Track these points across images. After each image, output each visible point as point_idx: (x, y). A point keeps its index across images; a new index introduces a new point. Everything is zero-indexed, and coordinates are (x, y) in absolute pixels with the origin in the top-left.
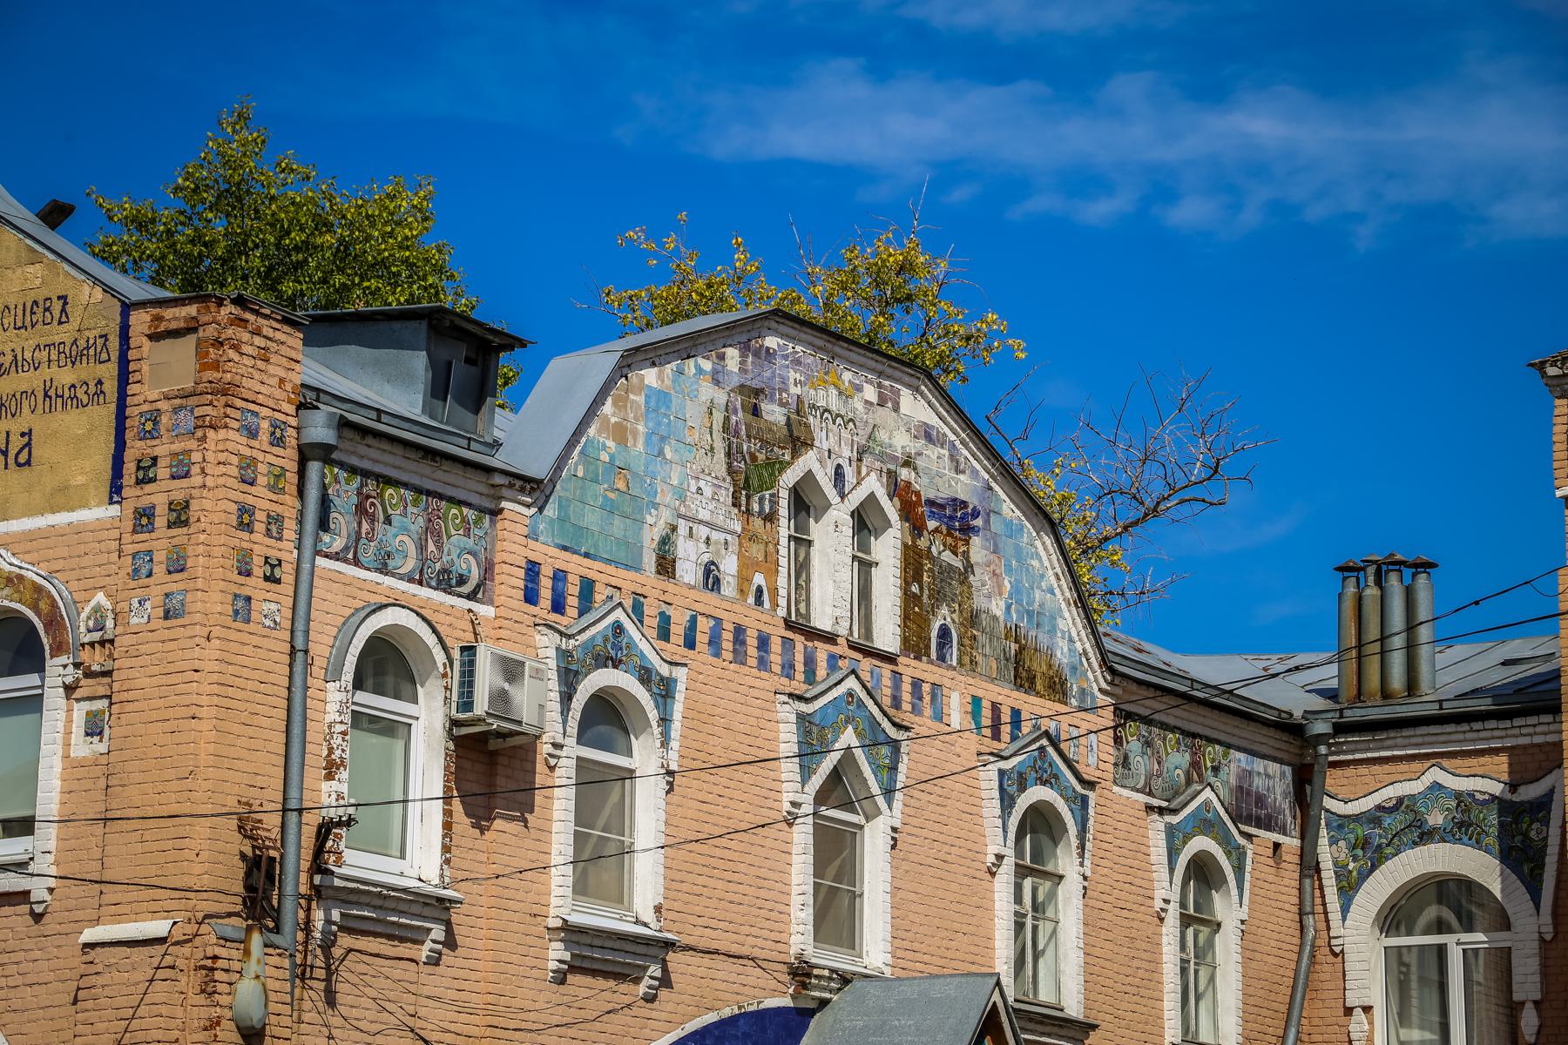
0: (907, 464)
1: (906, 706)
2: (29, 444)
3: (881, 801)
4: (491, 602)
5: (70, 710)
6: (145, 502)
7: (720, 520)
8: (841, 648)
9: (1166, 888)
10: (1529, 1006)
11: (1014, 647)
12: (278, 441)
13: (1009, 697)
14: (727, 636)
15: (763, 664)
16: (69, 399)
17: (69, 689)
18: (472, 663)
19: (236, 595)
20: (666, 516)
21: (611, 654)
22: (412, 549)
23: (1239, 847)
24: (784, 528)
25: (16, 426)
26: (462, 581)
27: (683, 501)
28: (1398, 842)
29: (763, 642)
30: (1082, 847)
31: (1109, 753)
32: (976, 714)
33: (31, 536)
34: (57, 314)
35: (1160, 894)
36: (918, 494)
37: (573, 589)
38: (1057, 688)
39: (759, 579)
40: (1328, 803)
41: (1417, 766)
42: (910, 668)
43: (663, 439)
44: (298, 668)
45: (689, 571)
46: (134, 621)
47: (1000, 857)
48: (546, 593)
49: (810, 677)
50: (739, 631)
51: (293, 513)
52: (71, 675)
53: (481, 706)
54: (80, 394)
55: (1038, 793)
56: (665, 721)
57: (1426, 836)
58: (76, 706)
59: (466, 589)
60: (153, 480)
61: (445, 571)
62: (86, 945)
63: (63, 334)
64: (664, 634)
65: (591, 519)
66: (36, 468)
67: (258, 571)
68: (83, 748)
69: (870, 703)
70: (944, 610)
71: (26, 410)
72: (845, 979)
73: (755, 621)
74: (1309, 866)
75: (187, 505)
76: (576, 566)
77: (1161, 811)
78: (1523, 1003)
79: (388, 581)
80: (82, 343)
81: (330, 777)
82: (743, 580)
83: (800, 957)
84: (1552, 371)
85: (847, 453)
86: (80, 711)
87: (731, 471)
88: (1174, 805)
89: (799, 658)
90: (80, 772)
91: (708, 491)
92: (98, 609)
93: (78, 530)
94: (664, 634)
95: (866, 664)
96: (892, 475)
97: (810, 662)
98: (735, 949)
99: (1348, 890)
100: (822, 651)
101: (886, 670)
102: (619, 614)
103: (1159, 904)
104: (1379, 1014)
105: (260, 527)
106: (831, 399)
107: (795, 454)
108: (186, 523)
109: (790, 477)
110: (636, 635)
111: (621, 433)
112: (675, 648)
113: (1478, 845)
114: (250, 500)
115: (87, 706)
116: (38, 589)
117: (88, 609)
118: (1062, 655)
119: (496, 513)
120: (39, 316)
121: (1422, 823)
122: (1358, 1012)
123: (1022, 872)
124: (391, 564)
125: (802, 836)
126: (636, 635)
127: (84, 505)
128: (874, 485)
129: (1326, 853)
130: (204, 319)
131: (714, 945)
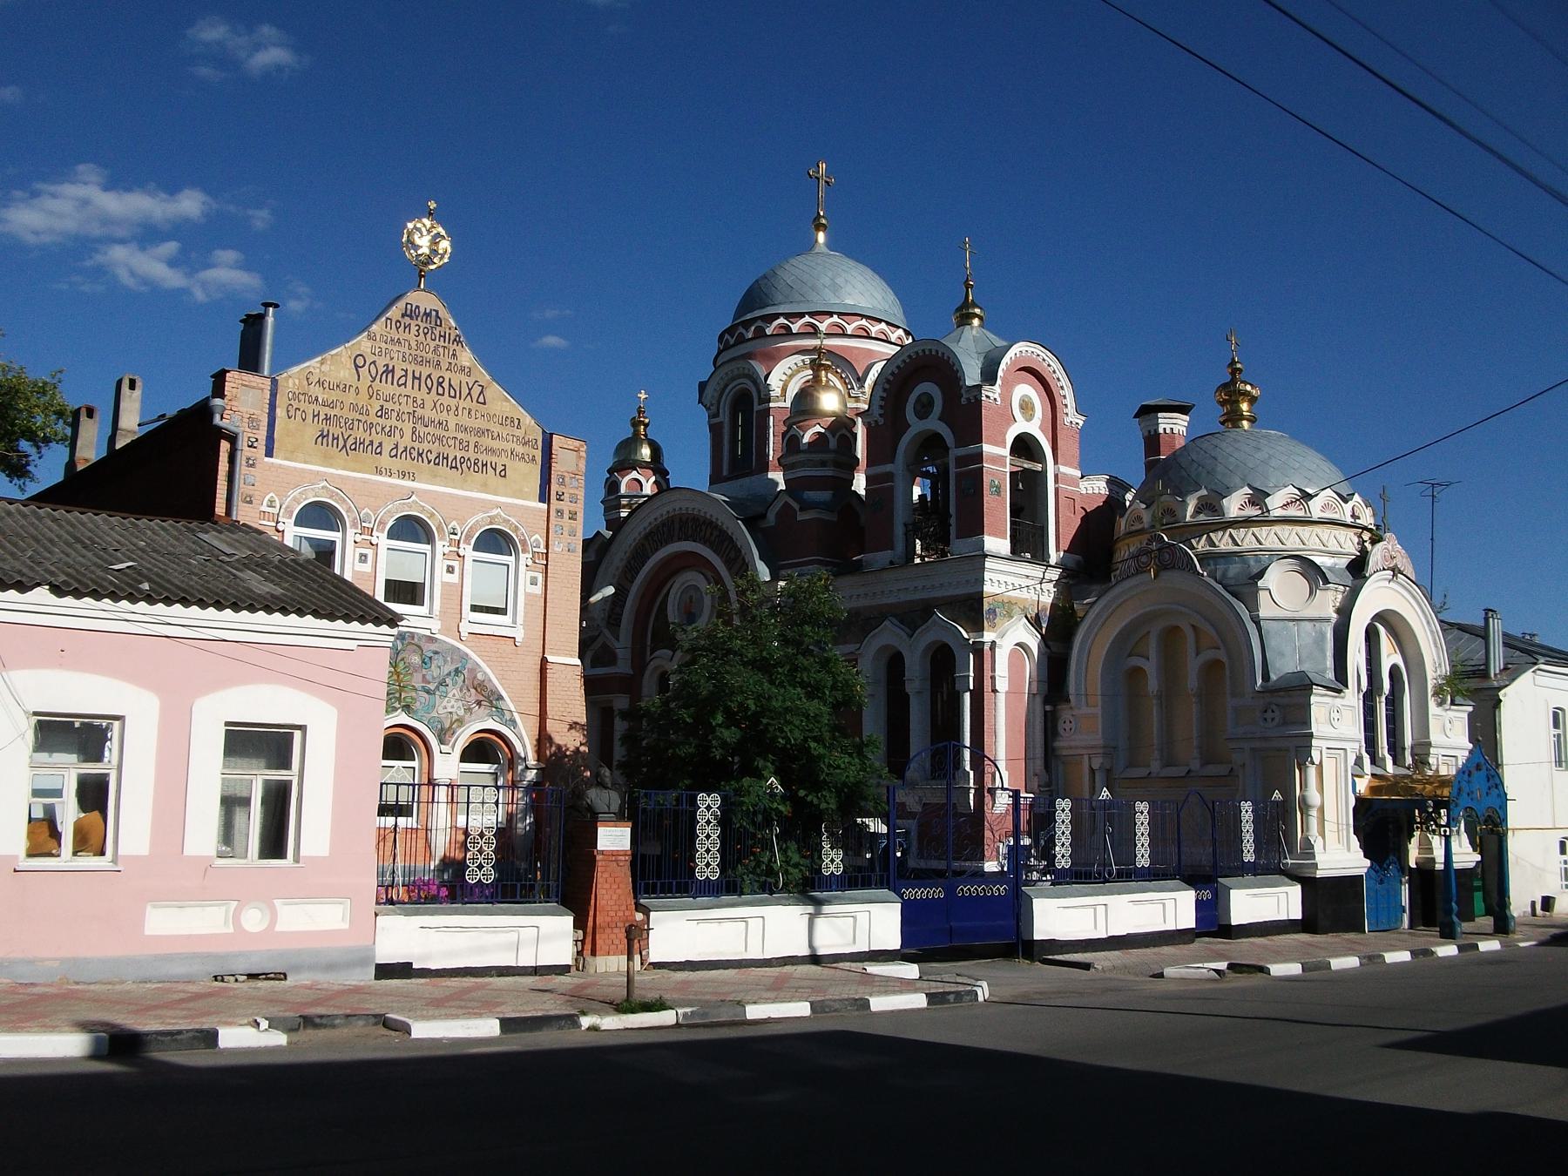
2: (505, 469)
6: (559, 507)
34: (516, 425)
54: (526, 457)
80: (527, 440)
92: (536, 540)
93: (527, 508)
108: (575, 520)
120: (509, 421)
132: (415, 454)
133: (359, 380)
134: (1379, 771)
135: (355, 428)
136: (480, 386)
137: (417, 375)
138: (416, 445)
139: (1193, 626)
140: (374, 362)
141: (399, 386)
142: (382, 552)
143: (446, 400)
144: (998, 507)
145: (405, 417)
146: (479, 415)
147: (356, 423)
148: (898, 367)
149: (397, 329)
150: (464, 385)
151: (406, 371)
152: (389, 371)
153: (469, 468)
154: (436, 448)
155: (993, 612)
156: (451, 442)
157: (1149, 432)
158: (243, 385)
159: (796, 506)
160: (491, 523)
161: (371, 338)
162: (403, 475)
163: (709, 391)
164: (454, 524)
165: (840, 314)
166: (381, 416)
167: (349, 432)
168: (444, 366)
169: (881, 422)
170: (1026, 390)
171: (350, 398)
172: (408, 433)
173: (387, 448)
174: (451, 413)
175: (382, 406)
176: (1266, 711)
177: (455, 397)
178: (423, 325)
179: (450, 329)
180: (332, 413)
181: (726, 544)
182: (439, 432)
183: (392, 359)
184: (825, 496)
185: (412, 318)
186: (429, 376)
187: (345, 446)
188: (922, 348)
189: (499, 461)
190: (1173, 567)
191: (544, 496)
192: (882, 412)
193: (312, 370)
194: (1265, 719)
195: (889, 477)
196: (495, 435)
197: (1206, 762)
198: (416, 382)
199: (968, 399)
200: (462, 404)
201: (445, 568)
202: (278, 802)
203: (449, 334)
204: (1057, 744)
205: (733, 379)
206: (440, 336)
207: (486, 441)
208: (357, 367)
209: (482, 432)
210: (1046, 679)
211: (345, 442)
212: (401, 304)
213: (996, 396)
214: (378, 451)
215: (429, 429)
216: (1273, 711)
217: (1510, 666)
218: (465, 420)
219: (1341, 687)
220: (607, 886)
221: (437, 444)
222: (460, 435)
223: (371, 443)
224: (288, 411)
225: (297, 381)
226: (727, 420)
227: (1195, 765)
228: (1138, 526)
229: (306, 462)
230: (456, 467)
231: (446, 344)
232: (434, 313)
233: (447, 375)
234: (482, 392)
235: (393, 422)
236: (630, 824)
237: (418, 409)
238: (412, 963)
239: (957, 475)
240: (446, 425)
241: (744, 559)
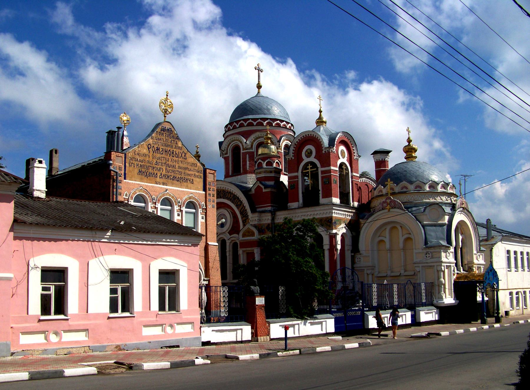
2: (193, 181)
63: (196, 168)
92: (203, 204)
93: (200, 194)
132: (167, 177)
134: (459, 272)
135: (149, 169)
137: (166, 150)
138: (167, 174)
139: (401, 227)
140: (154, 146)
141: (161, 154)
142: (159, 209)
143: (175, 158)
144: (336, 188)
145: (164, 164)
147: (149, 167)
148: (299, 140)
150: (180, 153)
151: (163, 149)
152: (158, 149)
155: (335, 223)
156: (177, 172)
157: (377, 160)
158: (116, 156)
159: (263, 187)
160: (190, 199)
161: (152, 138)
163: (224, 146)
164: (179, 199)
165: (271, 119)
168: (174, 147)
169: (293, 158)
170: (342, 148)
173: (159, 175)
174: (177, 163)
175: (156, 161)
176: (427, 254)
177: (177, 157)
178: (167, 133)
180: (142, 164)
181: (236, 200)
182: (173, 169)
184: (272, 183)
185: (164, 131)
186: (170, 150)
187: (146, 175)
188: (311, 133)
190: (395, 208)
191: (205, 189)
192: (293, 155)
193: (135, 150)
194: (426, 257)
195: (297, 177)
196: (190, 169)
197: (405, 271)
198: (166, 152)
199: (325, 151)
200: (180, 159)
202: (127, 295)
204: (355, 266)
205: (233, 141)
208: (149, 148)
209: (186, 169)
210: (351, 245)
211: (146, 173)
212: (160, 127)
214: (156, 176)
215: (171, 168)
216: (429, 254)
217: (494, 237)
218: (181, 165)
219: (449, 246)
220: (259, 316)
222: (179, 170)
224: (129, 164)
226: (230, 156)
227: (402, 272)
228: (381, 194)
229: (135, 181)
230: (179, 181)
232: (170, 129)
233: (175, 150)
234: (185, 155)
235: (160, 167)
236: (264, 296)
237: (167, 162)
238: (210, 341)
239: (322, 177)
241: (243, 205)
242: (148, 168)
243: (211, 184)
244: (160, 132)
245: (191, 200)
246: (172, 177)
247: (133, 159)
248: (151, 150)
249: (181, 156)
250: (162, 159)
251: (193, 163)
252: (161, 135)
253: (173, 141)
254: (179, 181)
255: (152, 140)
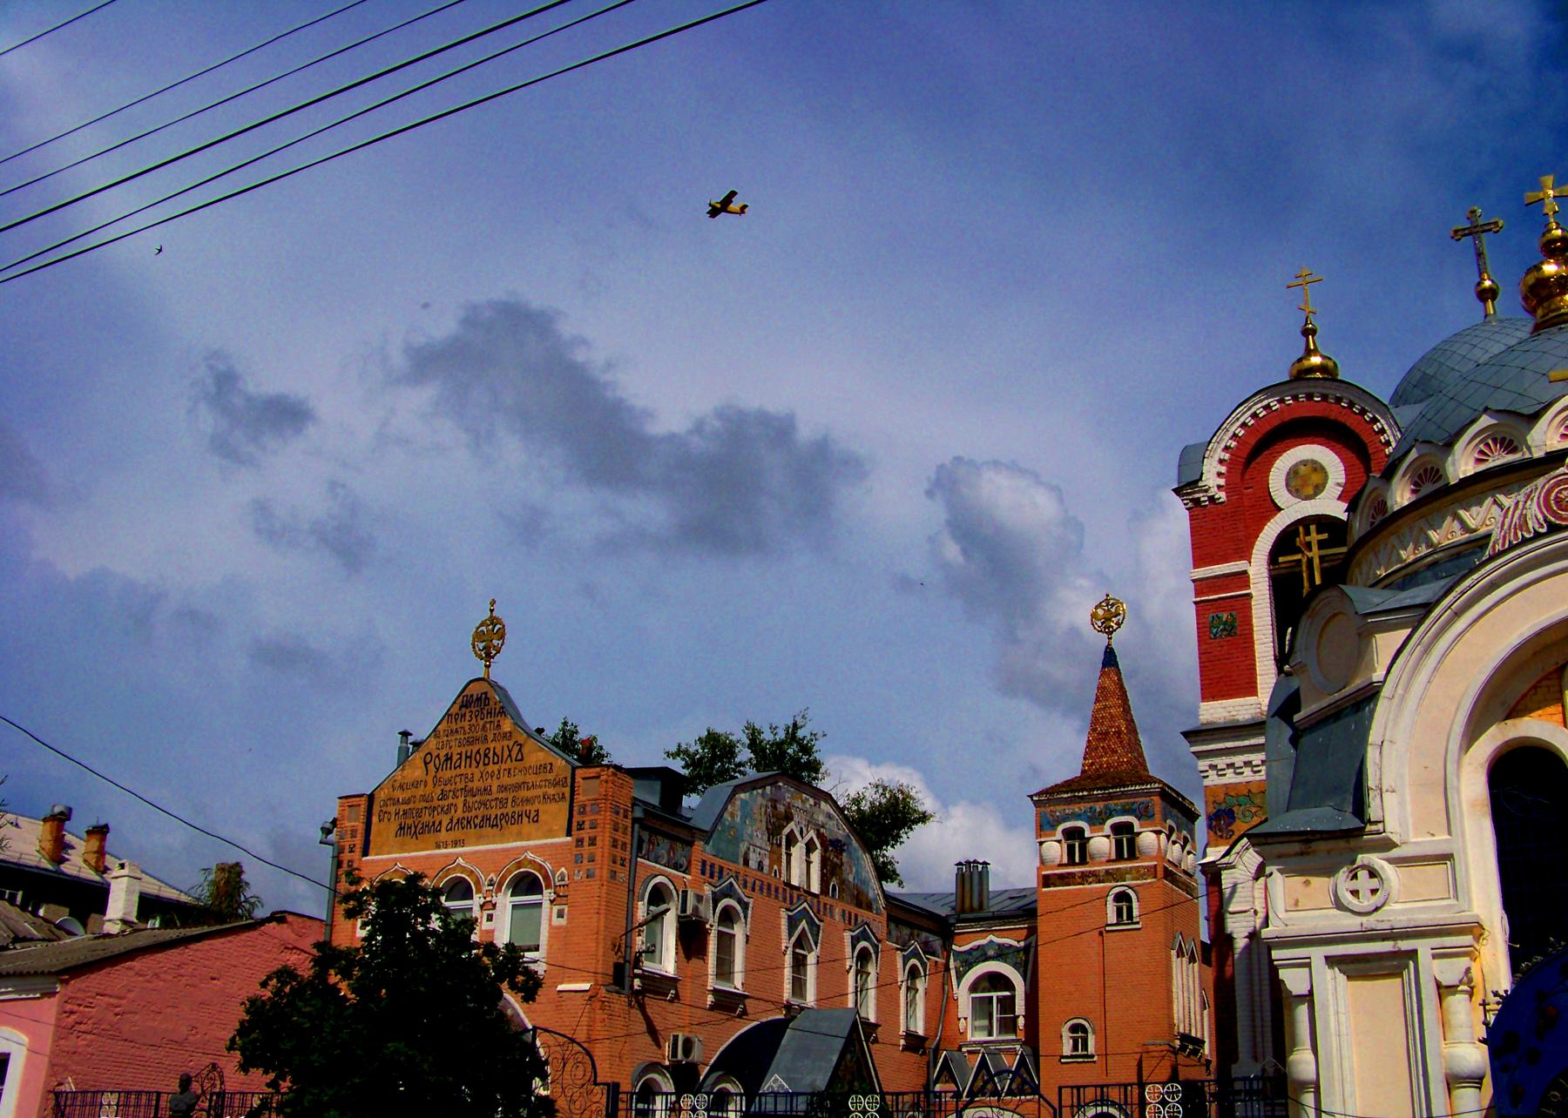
0: (823, 827)
1: (822, 913)
2: (537, 815)
3: (814, 947)
4: (690, 874)
5: (551, 909)
7: (763, 846)
8: (802, 893)
9: (901, 976)
10: (1021, 1017)
11: (856, 892)
12: (626, 817)
13: (854, 910)
14: (765, 887)
15: (777, 898)
16: (553, 799)
17: (552, 902)
18: (686, 896)
19: (612, 871)
20: (746, 844)
21: (729, 892)
22: (666, 855)
23: (925, 963)
24: (784, 850)
25: (534, 808)
26: (681, 866)
27: (752, 839)
28: (977, 962)
29: (777, 890)
30: (877, 963)
31: (885, 930)
32: (844, 915)
33: (537, 847)
34: (548, 768)
35: (900, 979)
36: (826, 837)
37: (717, 870)
38: (869, 907)
39: (775, 867)
40: (954, 947)
41: (984, 934)
42: (823, 899)
43: (746, 818)
44: (631, 895)
45: (753, 864)
46: (576, 878)
47: (851, 967)
48: (708, 872)
49: (791, 903)
50: (769, 885)
51: (630, 842)
52: (553, 896)
53: (689, 911)
54: (556, 797)
55: (863, 944)
56: (746, 917)
57: (988, 959)
58: (554, 907)
59: (682, 869)
60: (583, 829)
61: (676, 863)
62: (559, 991)
63: (551, 777)
64: (745, 887)
65: (723, 846)
66: (540, 823)
67: (619, 862)
68: (557, 921)
69: (811, 912)
70: (834, 879)
71: (537, 803)
72: (802, 1009)
73: (774, 883)
74: (947, 969)
75: (595, 838)
76: (718, 861)
77: (902, 950)
78: (1018, 1016)
79: (658, 866)
81: (639, 935)
82: (771, 867)
83: (787, 1002)
84: (1035, 798)
85: (804, 823)
86: (556, 909)
87: (767, 829)
88: (906, 948)
89: (788, 895)
90: (555, 931)
91: (760, 836)
92: (562, 873)
94: (745, 887)
95: (809, 898)
96: (818, 831)
97: (791, 897)
98: (767, 998)
99: (960, 977)
100: (795, 893)
101: (815, 900)
102: (732, 879)
103: (899, 984)
104: (969, 1020)
105: (619, 847)
106: (798, 803)
107: (788, 824)
108: (595, 845)
109: (786, 831)
110: (737, 887)
111: (732, 815)
112: (748, 891)
113: (1006, 962)
114: (616, 837)
115: (558, 907)
116: (541, 865)
117: (558, 873)
118: (871, 895)
119: (691, 844)
121: (986, 954)
122: (962, 1020)
123: (857, 972)
124: (660, 860)
125: (788, 959)
126: (737, 887)
127: (558, 837)
128: (812, 834)
129: (952, 964)
130: (602, 773)
131: (760, 997)
132: (465, 822)
133: (427, 774)
136: (518, 745)
137: (469, 754)
138: (466, 815)
140: (438, 756)
141: (455, 768)
143: (491, 768)
146: (517, 771)
147: (424, 810)
149: (456, 720)
150: (506, 748)
151: (461, 754)
153: (507, 823)
154: (482, 812)
156: (493, 803)
162: (456, 844)
166: (441, 799)
167: (419, 819)
168: (490, 737)
171: (421, 791)
172: (460, 806)
173: (445, 824)
174: (495, 778)
177: (497, 763)
178: (474, 710)
179: (495, 704)
183: (450, 748)
185: (466, 707)
186: (478, 752)
187: (415, 832)
189: (532, 808)
198: (468, 760)
200: (504, 766)
201: (485, 917)
203: (495, 709)
206: (488, 713)
207: (524, 793)
209: (518, 787)
211: (416, 827)
213: (1213, 491)
218: (506, 780)
221: (482, 809)
222: (501, 795)
223: (434, 823)
224: (379, 816)
225: (386, 791)
231: (492, 719)
232: (484, 696)
233: (492, 746)
234: (520, 750)
235: (450, 801)
240: (490, 790)
242: (419, 813)
243: (588, 809)
244: (457, 714)
245: (522, 870)
246: (480, 818)
247: (389, 802)
248: (431, 766)
249: (510, 755)
250: (458, 779)
251: (543, 763)
252: (458, 721)
253: (488, 726)
254: (497, 825)
255: (435, 742)
